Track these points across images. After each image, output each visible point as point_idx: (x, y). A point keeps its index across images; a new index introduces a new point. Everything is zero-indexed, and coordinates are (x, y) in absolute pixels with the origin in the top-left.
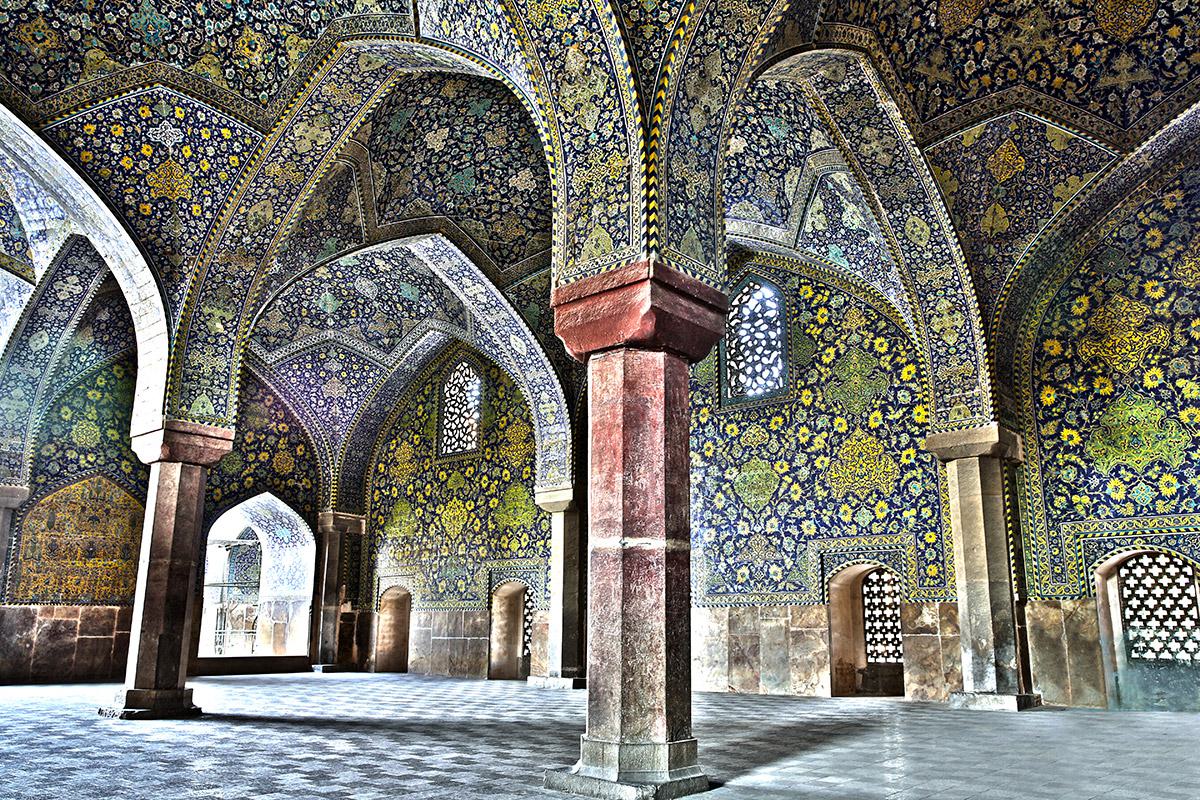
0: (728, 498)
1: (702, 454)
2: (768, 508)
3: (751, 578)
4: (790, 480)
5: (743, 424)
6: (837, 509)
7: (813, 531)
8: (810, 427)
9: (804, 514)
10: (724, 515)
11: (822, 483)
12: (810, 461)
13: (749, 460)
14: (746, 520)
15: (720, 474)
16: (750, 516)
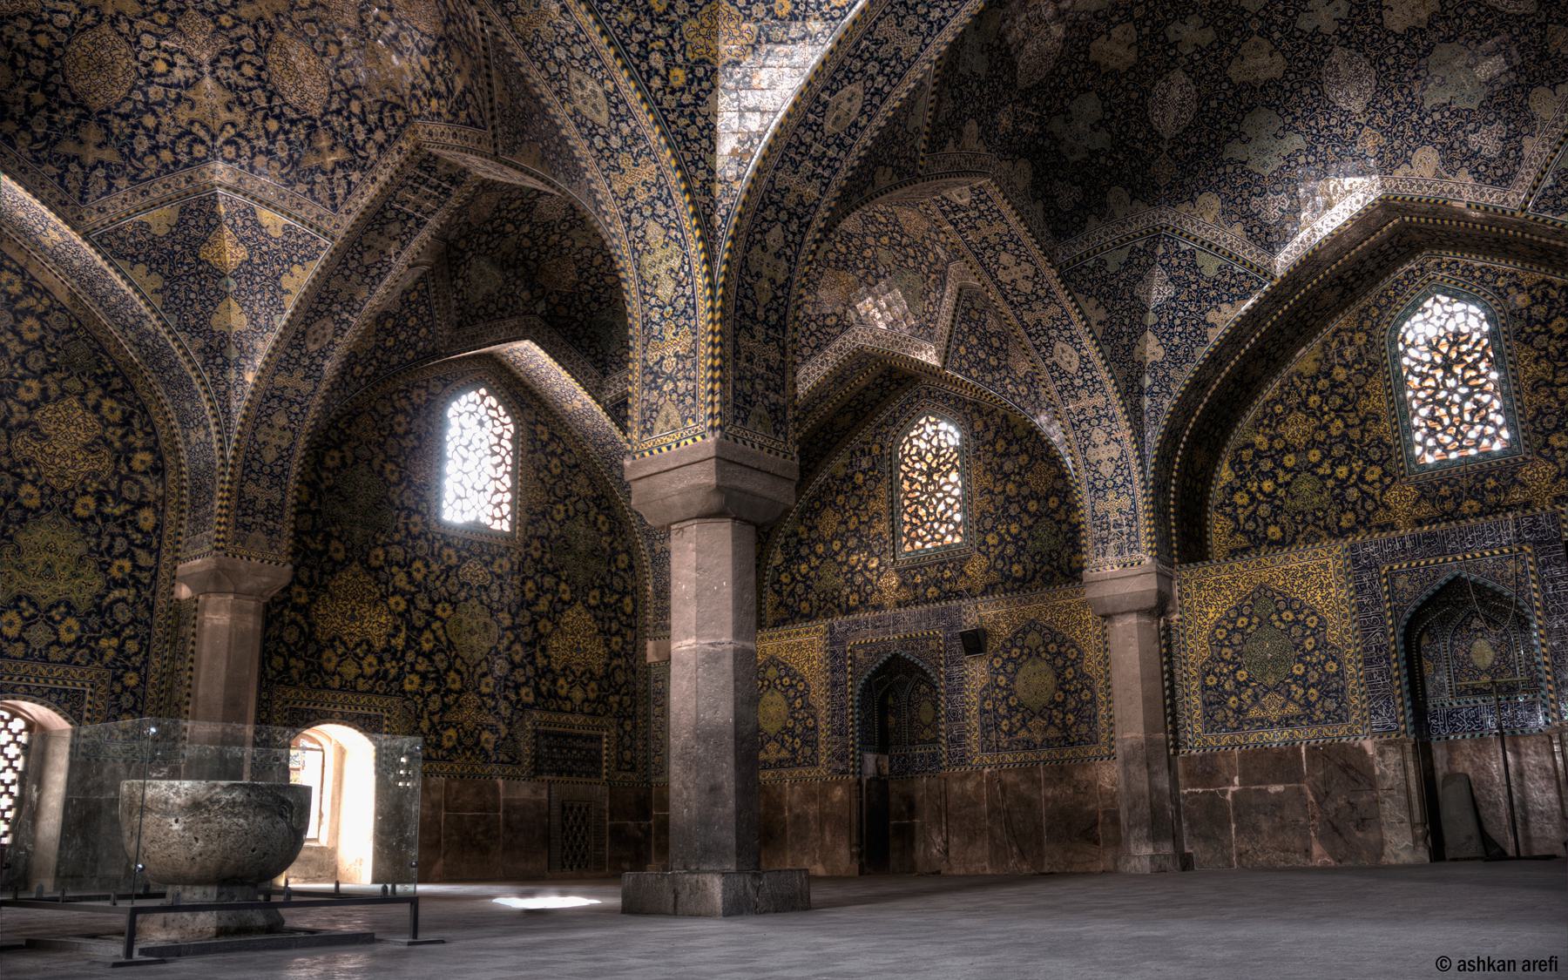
0: (437, 639)
1: (409, 574)
2: (484, 664)
3: (460, 743)
4: (512, 637)
5: (464, 553)
6: (554, 682)
7: (531, 699)
8: (536, 583)
9: (523, 679)
10: (432, 661)
11: (544, 649)
12: (534, 622)
13: (466, 600)
14: (458, 672)
15: (429, 607)
16: (463, 669)
